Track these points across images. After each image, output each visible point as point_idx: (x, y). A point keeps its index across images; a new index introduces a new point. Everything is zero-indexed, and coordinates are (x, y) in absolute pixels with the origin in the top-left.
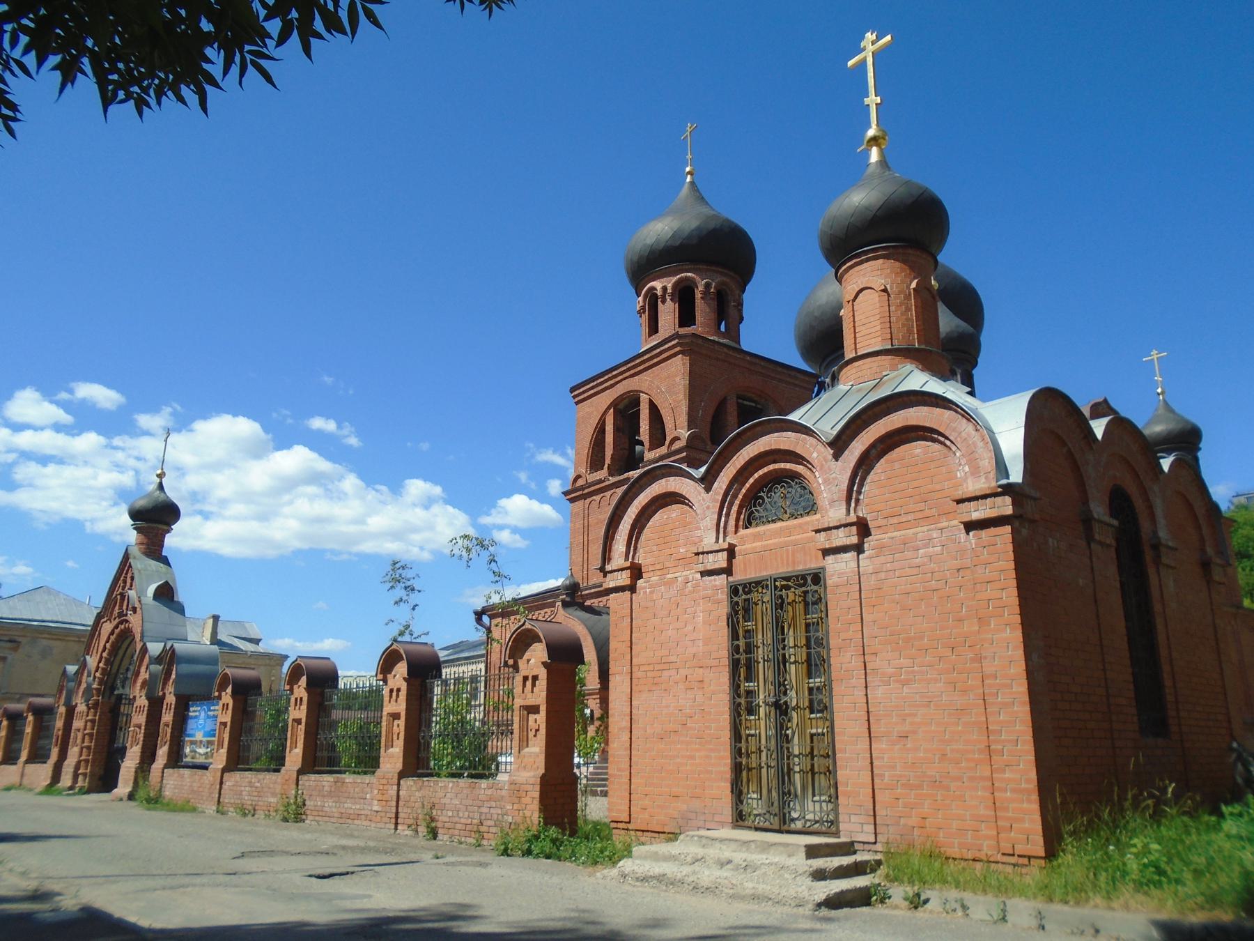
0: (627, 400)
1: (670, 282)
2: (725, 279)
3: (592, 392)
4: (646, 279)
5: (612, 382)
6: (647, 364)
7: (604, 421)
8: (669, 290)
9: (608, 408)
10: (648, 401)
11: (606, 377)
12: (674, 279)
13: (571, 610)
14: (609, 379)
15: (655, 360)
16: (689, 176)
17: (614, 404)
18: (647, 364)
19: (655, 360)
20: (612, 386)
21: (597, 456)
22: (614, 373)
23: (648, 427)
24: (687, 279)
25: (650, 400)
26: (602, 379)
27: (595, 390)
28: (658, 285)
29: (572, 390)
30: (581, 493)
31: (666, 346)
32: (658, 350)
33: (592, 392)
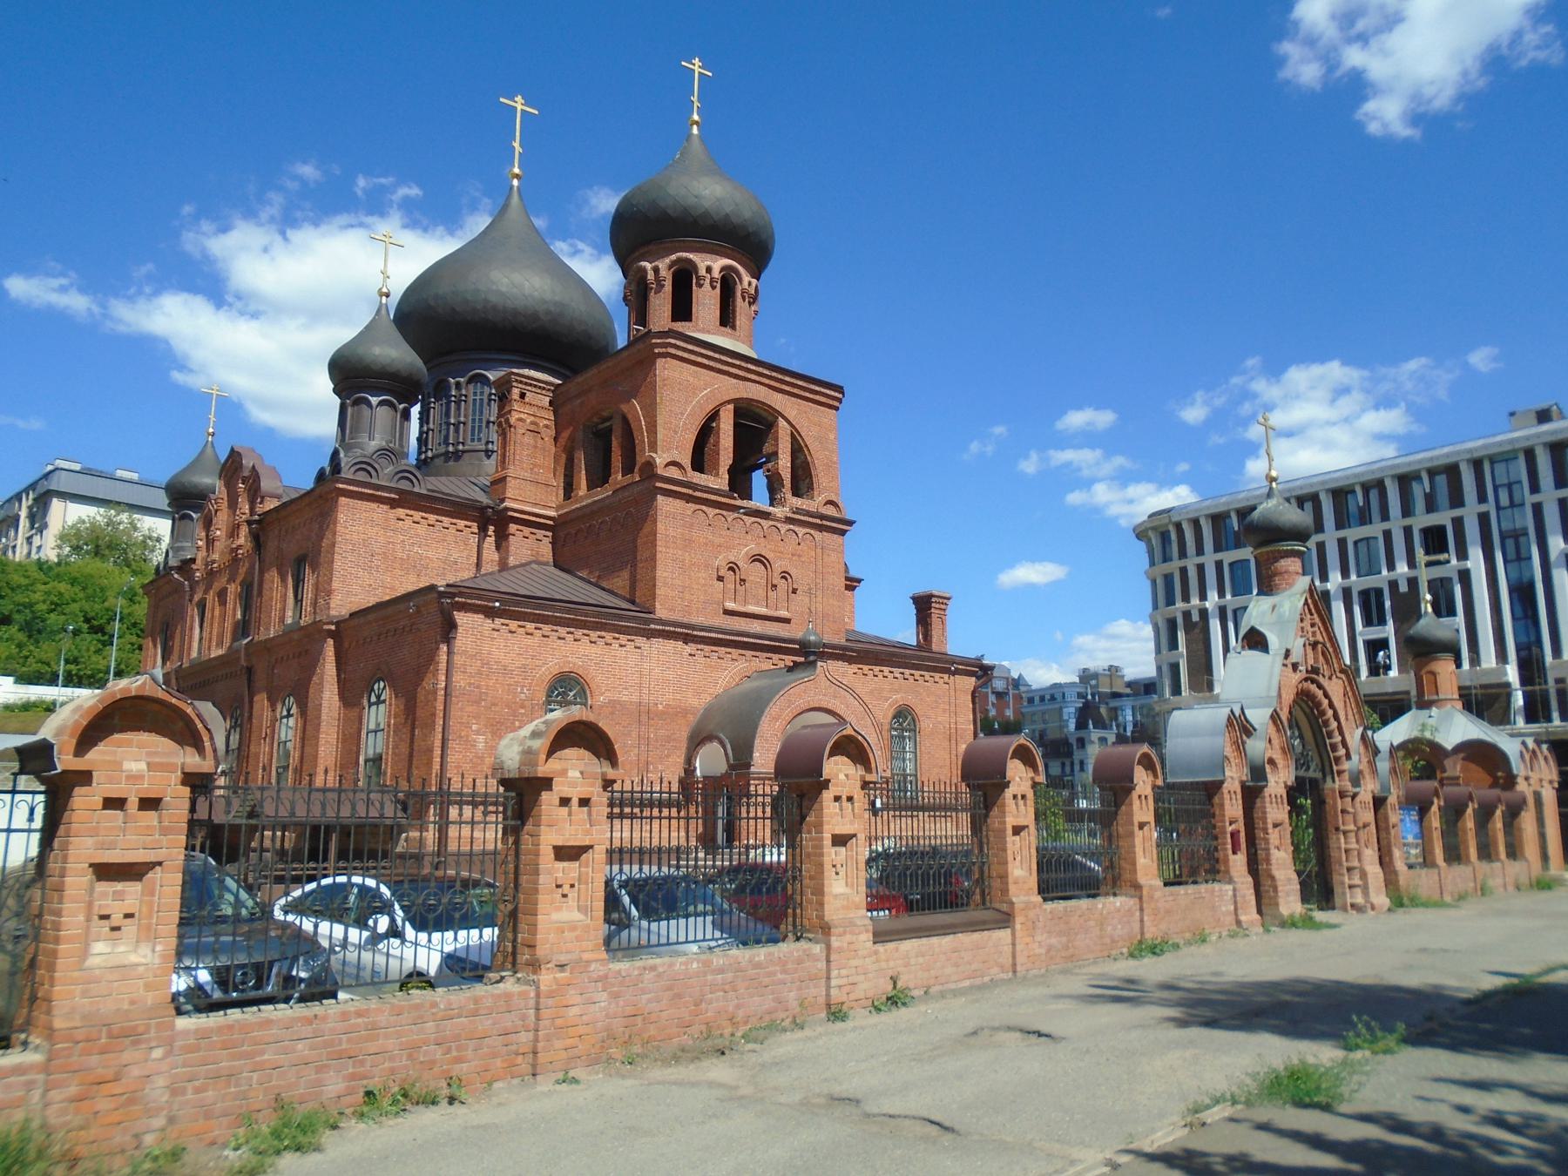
4: (740, 256)
5: (741, 373)
6: (796, 391)
9: (729, 402)
11: (738, 362)
14: (739, 367)
15: (807, 395)
16: (695, 127)
18: (796, 391)
19: (807, 395)
22: (787, 379)
23: (789, 464)
25: (792, 433)
26: (730, 360)
27: (712, 364)
30: (690, 492)
31: (828, 392)
32: (817, 388)
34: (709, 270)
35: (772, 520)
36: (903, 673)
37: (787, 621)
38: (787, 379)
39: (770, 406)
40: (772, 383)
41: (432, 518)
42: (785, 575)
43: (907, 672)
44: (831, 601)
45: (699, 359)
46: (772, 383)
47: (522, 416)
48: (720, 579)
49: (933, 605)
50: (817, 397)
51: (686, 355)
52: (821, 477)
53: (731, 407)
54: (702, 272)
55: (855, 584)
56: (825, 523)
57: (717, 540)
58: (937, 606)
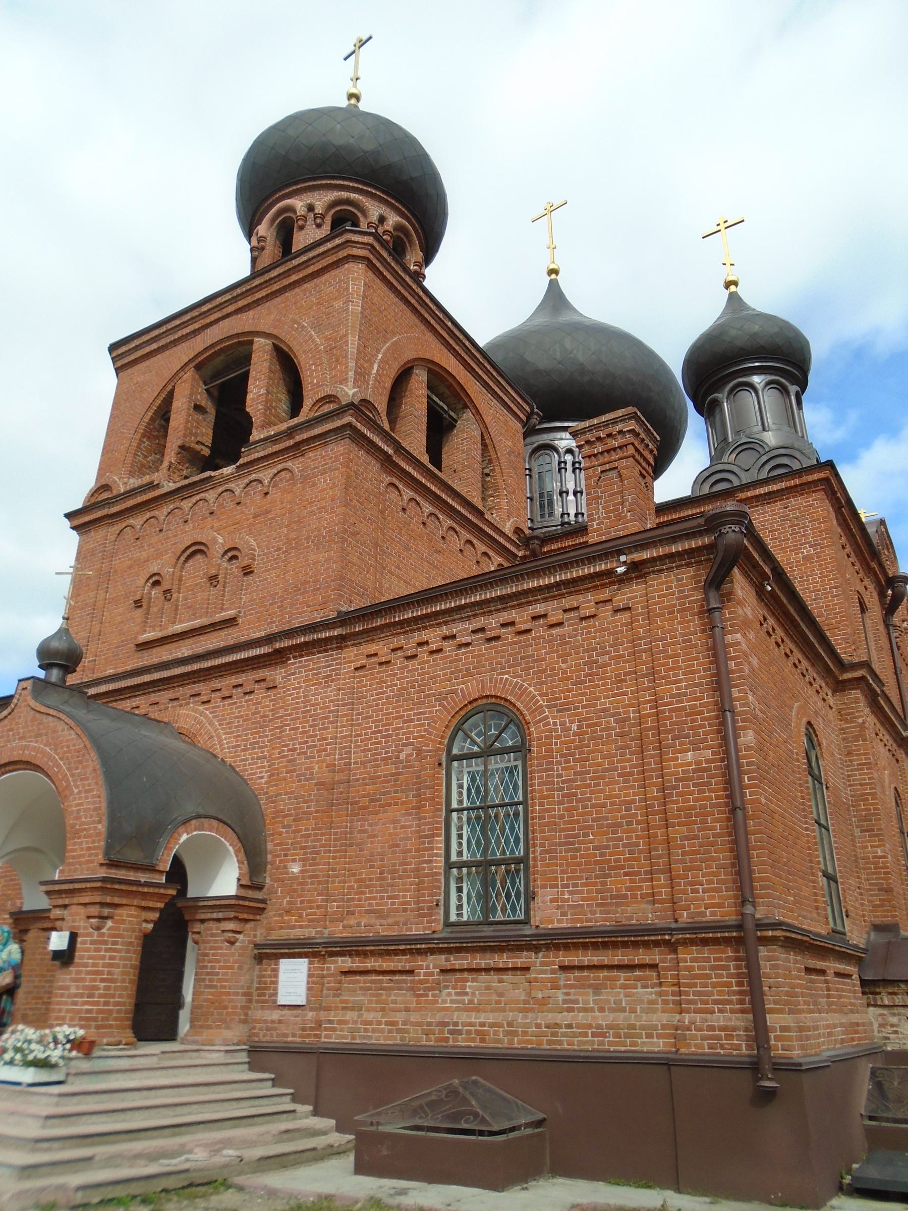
0: (222, 358)
2: (404, 221)
3: (154, 346)
5: (196, 326)
7: (171, 395)
9: (182, 368)
10: (269, 347)
13: (54, 698)
15: (294, 278)
17: (200, 365)
18: (276, 287)
20: (196, 332)
21: (145, 457)
24: (348, 202)
28: (299, 204)
29: (113, 348)
33: (154, 346)
37: (231, 622)
39: (238, 335)
40: (241, 304)
42: (232, 554)
43: (492, 622)
44: (312, 557)
45: (148, 349)
46: (241, 304)
48: (138, 604)
51: (132, 357)
53: (190, 374)
56: (298, 438)
57: (144, 555)
58: (600, 448)
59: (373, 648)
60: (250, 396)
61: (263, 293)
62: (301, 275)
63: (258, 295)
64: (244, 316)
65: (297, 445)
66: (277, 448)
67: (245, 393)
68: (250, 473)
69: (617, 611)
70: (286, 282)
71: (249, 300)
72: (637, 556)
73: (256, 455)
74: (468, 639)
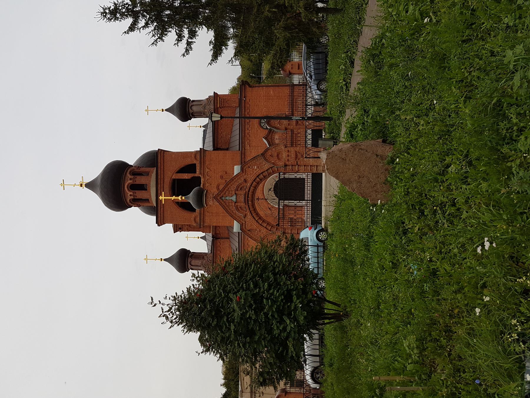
1: (129, 176)
8: (132, 177)
12: (128, 174)
15: (162, 167)
18: (162, 172)
23: (186, 174)
24: (130, 172)
33: (162, 209)
34: (131, 195)
35: (205, 182)
36: (248, 123)
38: (159, 177)
41: (218, 252)
46: (162, 182)
47: (186, 228)
49: (223, 106)
50: (162, 163)
52: (189, 161)
54: (132, 197)
55: (216, 95)
59: (247, 143)
60: (186, 178)
61: (162, 176)
62: (162, 166)
63: (162, 178)
64: (165, 181)
65: (204, 162)
66: (202, 167)
67: (185, 179)
68: (205, 175)
69: (250, 101)
70: (162, 170)
71: (162, 180)
72: (243, 96)
73: (202, 172)
74: (249, 125)
